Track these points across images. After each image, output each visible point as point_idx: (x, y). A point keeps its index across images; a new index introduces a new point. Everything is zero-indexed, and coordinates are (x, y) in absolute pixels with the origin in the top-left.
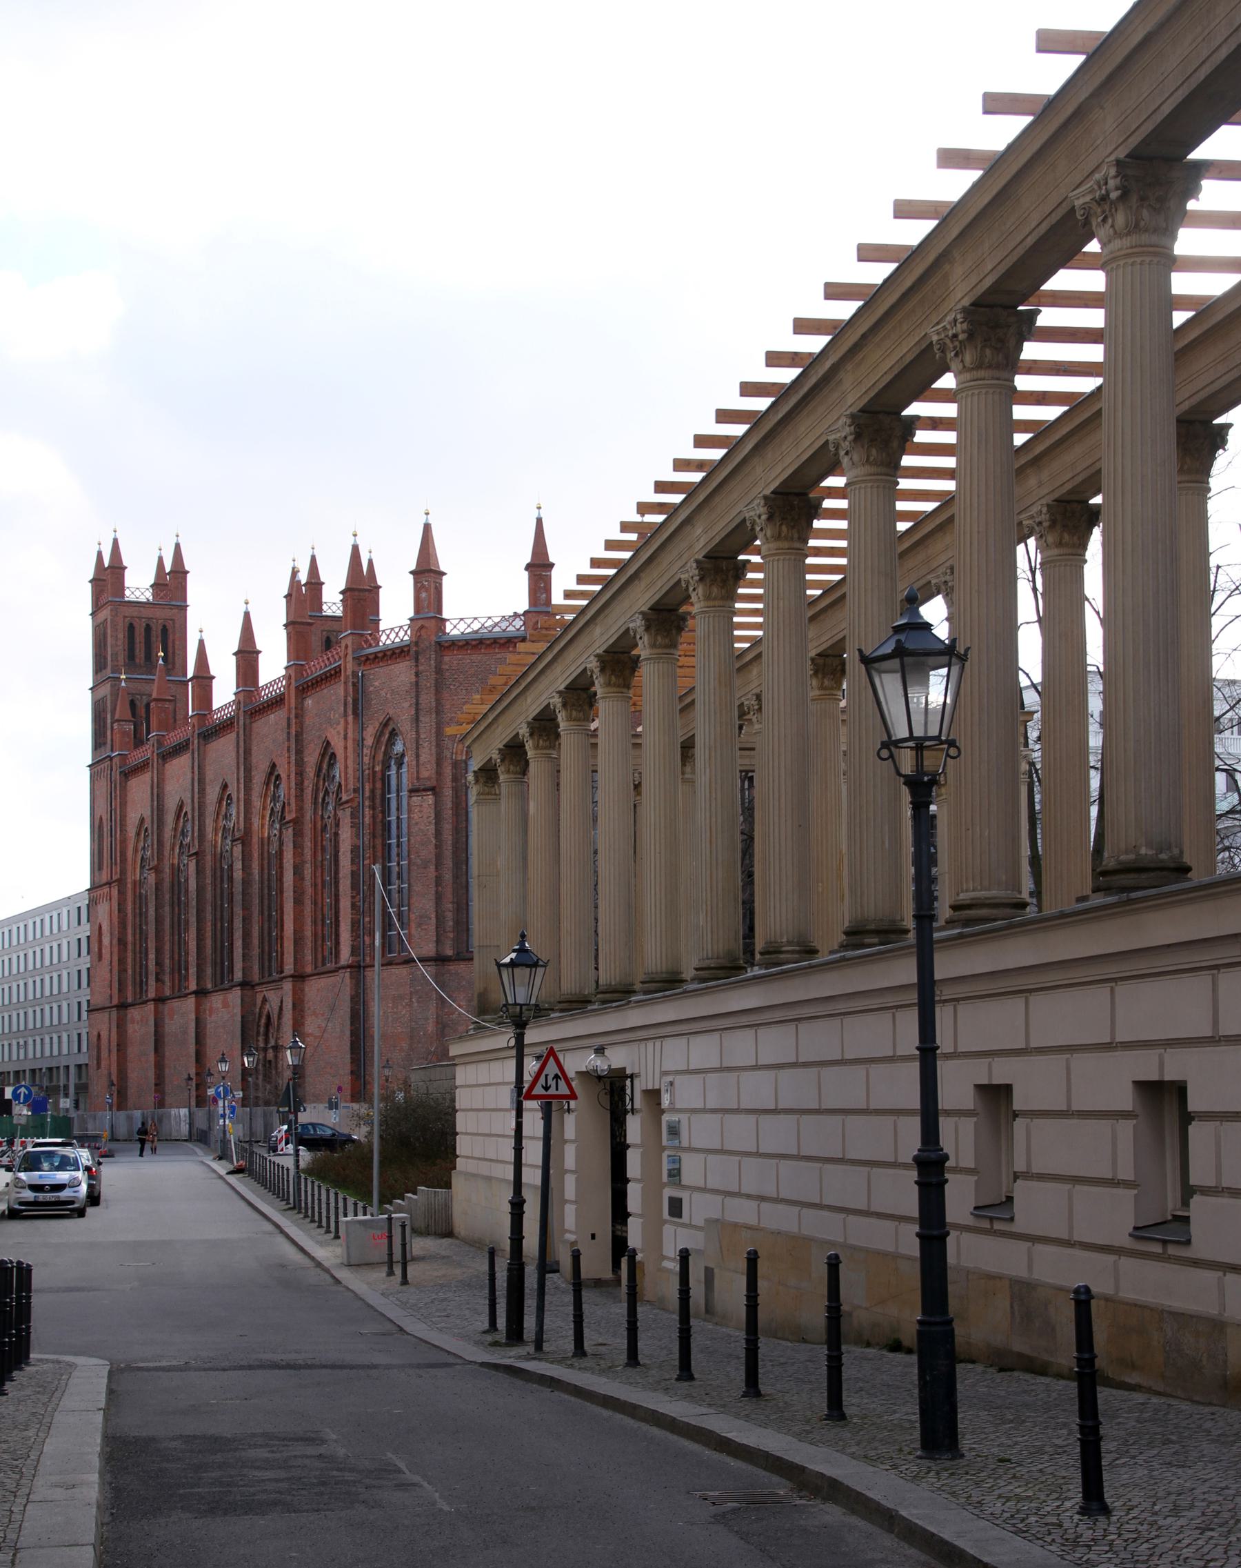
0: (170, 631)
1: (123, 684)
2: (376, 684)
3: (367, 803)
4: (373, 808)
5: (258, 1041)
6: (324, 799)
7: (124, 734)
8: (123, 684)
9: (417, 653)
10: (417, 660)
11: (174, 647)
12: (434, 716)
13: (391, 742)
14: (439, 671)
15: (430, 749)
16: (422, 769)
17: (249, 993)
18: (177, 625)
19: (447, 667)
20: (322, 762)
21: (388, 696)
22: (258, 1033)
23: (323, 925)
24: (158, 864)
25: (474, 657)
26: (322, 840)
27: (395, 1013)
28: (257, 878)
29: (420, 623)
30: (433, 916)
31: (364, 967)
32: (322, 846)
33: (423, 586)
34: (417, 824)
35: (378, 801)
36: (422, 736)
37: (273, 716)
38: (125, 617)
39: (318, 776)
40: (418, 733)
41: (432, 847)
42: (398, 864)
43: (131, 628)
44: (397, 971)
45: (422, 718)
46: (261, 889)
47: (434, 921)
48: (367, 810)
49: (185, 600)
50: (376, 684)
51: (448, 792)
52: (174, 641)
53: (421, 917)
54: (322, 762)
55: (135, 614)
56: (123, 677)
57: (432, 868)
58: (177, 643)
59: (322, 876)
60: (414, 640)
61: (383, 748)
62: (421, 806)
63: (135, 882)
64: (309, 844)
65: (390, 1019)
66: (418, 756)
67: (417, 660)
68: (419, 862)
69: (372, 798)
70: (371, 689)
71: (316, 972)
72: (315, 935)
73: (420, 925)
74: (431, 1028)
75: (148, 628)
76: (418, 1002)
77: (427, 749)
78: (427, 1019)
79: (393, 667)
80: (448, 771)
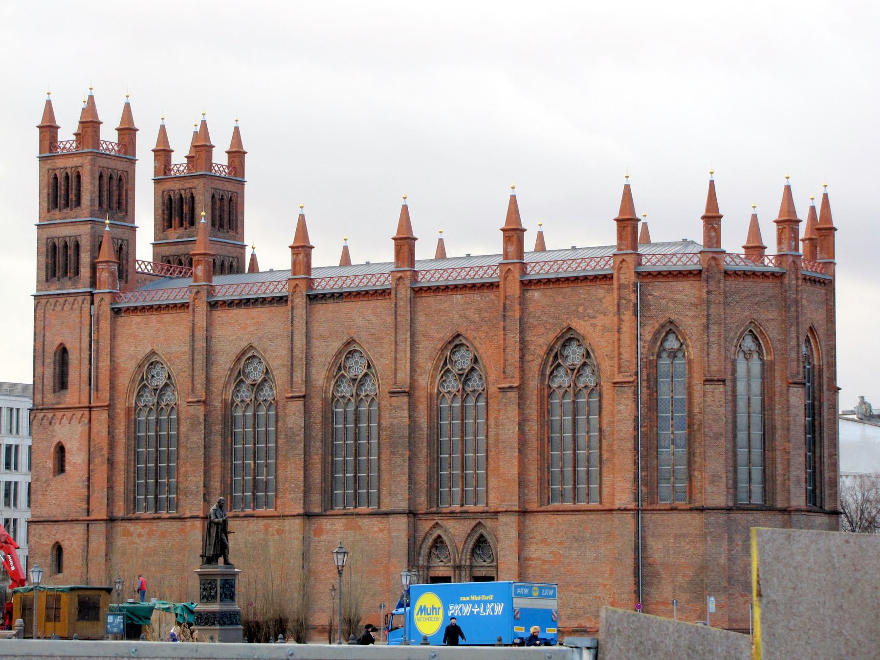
0: (124, 181)
1: (107, 228)
2: (655, 294)
3: (645, 384)
4: (648, 388)
5: (419, 560)
6: (552, 372)
7: (112, 273)
8: (107, 228)
9: (708, 277)
10: (708, 282)
11: (127, 195)
12: (723, 325)
13: (664, 340)
14: (725, 292)
15: (719, 350)
16: (712, 364)
17: (412, 520)
18: (129, 177)
19: (728, 289)
20: (556, 343)
21: (670, 304)
22: (419, 554)
23: (548, 473)
24: (206, 398)
25: (746, 284)
26: (548, 404)
27: (678, 547)
28: (424, 425)
29: (711, 255)
30: (724, 476)
31: (642, 510)
32: (548, 409)
33: (713, 227)
34: (710, 405)
35: (652, 383)
36: (712, 339)
37: (459, 297)
38: (99, 167)
39: (548, 354)
40: (708, 337)
41: (722, 424)
42: (673, 433)
43: (101, 176)
44: (680, 516)
45: (711, 326)
46: (429, 436)
47: (724, 479)
48: (645, 390)
49: (134, 155)
50: (655, 294)
51: (729, 383)
52: (127, 190)
53: (713, 476)
54: (556, 343)
55: (105, 165)
56: (107, 222)
57: (723, 440)
58: (129, 192)
59: (548, 433)
60: (706, 266)
61: (659, 343)
62: (713, 392)
63: (129, 409)
64: (534, 406)
65: (671, 552)
66: (708, 354)
67: (708, 282)
68: (711, 434)
69: (648, 380)
70: (650, 297)
71: (542, 508)
72: (540, 479)
73: (712, 482)
74: (723, 561)
75: (111, 178)
76: (712, 540)
77: (715, 350)
78: (719, 554)
79: (675, 283)
80: (729, 367)
